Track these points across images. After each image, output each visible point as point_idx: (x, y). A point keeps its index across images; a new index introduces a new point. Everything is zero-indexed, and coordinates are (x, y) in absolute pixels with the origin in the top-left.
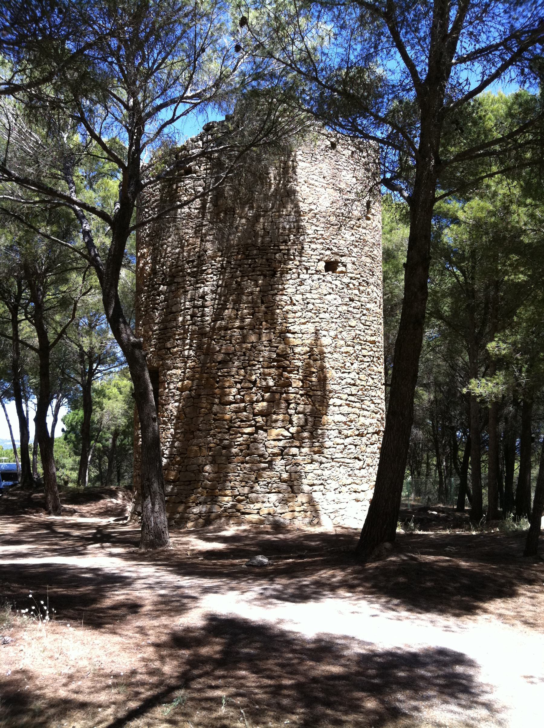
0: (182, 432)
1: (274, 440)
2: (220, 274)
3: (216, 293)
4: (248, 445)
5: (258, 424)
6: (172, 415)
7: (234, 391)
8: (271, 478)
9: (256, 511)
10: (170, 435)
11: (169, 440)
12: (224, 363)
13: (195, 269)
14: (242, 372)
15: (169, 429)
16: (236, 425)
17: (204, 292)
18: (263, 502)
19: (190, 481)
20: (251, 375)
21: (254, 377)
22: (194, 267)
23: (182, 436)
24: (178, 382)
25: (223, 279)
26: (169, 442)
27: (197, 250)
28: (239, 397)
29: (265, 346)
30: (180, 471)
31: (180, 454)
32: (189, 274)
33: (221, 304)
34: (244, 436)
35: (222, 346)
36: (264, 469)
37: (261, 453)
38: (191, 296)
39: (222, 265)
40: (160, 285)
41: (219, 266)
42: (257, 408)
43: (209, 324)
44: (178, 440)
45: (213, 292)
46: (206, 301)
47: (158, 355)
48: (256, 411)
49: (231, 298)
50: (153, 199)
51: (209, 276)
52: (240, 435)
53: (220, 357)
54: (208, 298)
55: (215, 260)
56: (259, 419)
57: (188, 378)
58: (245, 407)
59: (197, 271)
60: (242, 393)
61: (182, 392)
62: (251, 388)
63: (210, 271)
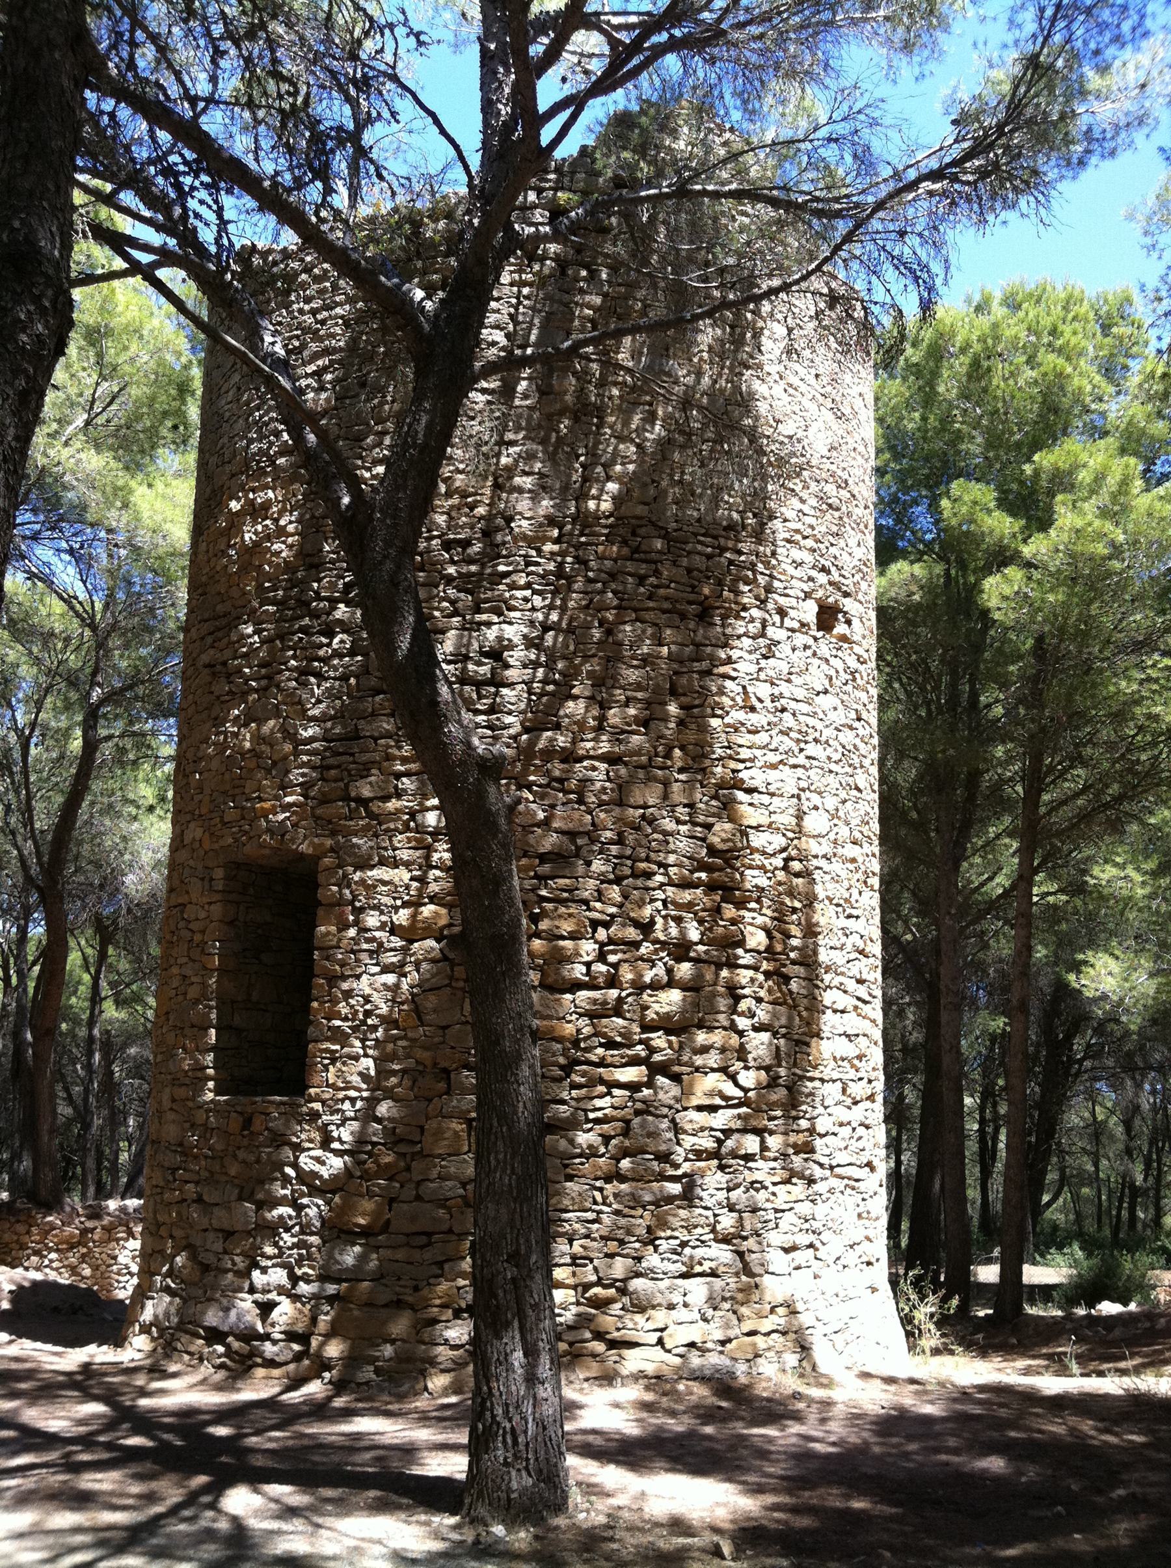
0: (404, 1071)
1: (700, 1108)
2: (555, 593)
3: (538, 647)
4: (627, 1122)
5: (657, 1058)
6: (368, 1014)
7: (588, 948)
8: (689, 1228)
9: (653, 1338)
10: (356, 1080)
11: (353, 1093)
12: (561, 860)
13: (473, 568)
14: (614, 892)
15: (356, 1058)
16: (594, 1058)
17: (500, 639)
18: (671, 1307)
19: (430, 1234)
20: (641, 904)
21: (647, 911)
22: (470, 561)
23: (407, 1082)
24: (396, 909)
25: (563, 609)
26: (353, 1101)
27: (481, 510)
28: (603, 968)
29: (679, 822)
30: (392, 1201)
31: (395, 1143)
32: (449, 580)
33: (555, 682)
34: (616, 1092)
35: (553, 806)
36: (670, 1199)
37: (663, 1147)
38: (458, 646)
39: (560, 566)
40: (334, 602)
41: (551, 566)
42: (656, 1007)
43: (515, 738)
44: (389, 1094)
45: (529, 643)
46: (507, 666)
47: (317, 818)
48: (651, 1015)
49: (588, 667)
50: (314, 347)
51: (519, 594)
52: (602, 1089)
53: (550, 842)
54: (515, 657)
55: (539, 551)
56: (659, 1040)
57: (433, 899)
58: (620, 1000)
59: (480, 573)
60: (612, 958)
61: (411, 941)
62: (636, 945)
63: (522, 580)
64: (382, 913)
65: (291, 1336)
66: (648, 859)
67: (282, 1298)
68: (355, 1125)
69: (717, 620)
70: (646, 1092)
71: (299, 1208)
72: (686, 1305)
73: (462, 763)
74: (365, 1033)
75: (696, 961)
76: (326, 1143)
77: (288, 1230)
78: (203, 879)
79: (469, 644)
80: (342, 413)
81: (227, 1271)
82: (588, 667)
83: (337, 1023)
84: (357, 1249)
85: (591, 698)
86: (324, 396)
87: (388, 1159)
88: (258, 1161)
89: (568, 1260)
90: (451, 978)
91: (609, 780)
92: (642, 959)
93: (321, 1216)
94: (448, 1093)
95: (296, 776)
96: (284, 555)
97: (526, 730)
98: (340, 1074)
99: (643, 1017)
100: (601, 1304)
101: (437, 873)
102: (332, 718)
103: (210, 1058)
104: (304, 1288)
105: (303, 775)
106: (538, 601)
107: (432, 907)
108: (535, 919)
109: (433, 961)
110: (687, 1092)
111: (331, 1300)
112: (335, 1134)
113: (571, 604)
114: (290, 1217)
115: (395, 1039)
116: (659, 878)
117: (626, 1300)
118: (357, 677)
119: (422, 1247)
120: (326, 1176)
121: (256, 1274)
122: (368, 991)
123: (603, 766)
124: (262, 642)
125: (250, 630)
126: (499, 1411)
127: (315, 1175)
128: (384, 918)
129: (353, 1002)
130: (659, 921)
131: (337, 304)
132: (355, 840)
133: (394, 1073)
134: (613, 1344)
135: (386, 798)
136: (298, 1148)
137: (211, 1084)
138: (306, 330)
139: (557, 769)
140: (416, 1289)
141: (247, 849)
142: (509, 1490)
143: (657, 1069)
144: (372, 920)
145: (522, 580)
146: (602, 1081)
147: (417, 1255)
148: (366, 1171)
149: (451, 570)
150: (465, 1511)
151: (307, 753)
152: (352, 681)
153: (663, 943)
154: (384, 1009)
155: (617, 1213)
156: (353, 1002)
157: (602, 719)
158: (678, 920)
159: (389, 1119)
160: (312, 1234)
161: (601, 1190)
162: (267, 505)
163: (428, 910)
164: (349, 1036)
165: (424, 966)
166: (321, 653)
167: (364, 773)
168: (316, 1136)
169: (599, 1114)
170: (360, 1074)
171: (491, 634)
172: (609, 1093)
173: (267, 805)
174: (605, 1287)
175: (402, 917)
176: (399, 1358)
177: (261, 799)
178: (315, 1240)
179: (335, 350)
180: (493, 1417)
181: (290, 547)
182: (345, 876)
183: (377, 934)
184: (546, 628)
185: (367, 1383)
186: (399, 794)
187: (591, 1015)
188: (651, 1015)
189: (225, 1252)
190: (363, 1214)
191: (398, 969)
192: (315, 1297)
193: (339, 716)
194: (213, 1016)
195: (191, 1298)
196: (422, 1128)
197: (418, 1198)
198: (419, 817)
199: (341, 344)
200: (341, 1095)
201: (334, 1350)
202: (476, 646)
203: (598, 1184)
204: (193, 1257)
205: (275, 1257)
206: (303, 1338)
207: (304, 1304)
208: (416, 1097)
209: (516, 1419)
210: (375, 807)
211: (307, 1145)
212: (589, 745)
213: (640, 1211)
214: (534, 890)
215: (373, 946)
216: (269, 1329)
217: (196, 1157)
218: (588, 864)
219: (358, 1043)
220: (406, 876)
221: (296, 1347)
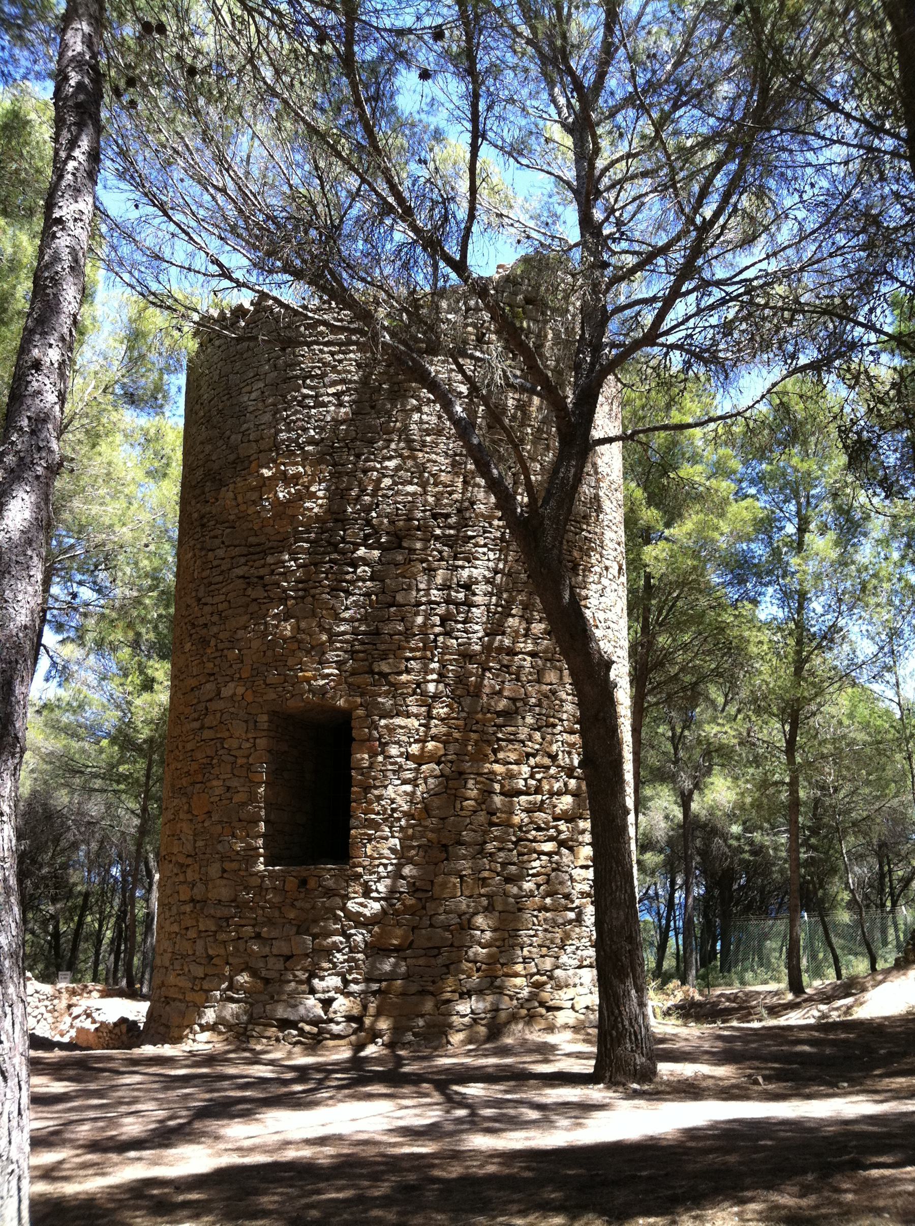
0: (419, 846)
1: (582, 867)
2: (500, 550)
3: (491, 583)
4: (548, 875)
5: (562, 836)
6: (394, 810)
7: (525, 770)
8: (579, 939)
9: (568, 1004)
10: (386, 852)
11: (385, 861)
12: (510, 715)
13: (452, 532)
14: (537, 736)
15: (386, 839)
16: (531, 837)
17: (470, 577)
18: (575, 986)
19: (439, 948)
20: (551, 743)
21: (554, 747)
22: (450, 528)
23: (421, 853)
24: (410, 744)
25: (506, 561)
26: (385, 866)
27: (455, 496)
28: (534, 782)
29: (568, 694)
30: (414, 929)
31: (415, 892)
32: (437, 538)
33: (501, 606)
34: (543, 857)
35: (503, 682)
36: (570, 922)
37: (566, 891)
38: (445, 580)
39: (503, 534)
40: (357, 546)
41: (498, 534)
42: (560, 806)
43: (480, 639)
44: (410, 861)
45: (488, 581)
46: (474, 594)
47: (350, 685)
48: (558, 811)
49: (520, 597)
50: (334, 376)
51: (481, 550)
52: (535, 856)
53: (503, 704)
54: (480, 588)
55: (491, 525)
56: (562, 825)
57: (434, 738)
58: (542, 802)
59: (457, 536)
60: (538, 776)
61: (420, 765)
62: (548, 768)
63: (481, 541)
64: (401, 746)
65: (349, 1019)
66: (554, 717)
67: (338, 995)
68: (388, 881)
69: (581, 572)
70: (556, 858)
71: (348, 937)
72: (581, 985)
73: (598, 664)
74: (392, 822)
75: (577, 778)
76: (367, 893)
77: (339, 951)
78: (246, 722)
79: (452, 579)
80: (358, 423)
81: (290, 981)
82: (520, 597)
83: (373, 816)
84: (392, 960)
85: (521, 617)
86: (343, 410)
87: (411, 902)
88: (313, 908)
89: (521, 960)
90: (446, 787)
91: (532, 667)
92: (552, 777)
93: (365, 941)
94: (447, 859)
95: (331, 656)
96: (315, 510)
97: (487, 635)
98: (375, 849)
99: (554, 812)
100: (539, 986)
101: (436, 722)
102: (358, 620)
103: (260, 842)
104: (354, 987)
105: (337, 656)
106: (491, 555)
107: (433, 743)
108: (495, 752)
109: (436, 777)
110: (576, 857)
111: (374, 993)
112: (374, 887)
113: (510, 558)
114: (341, 943)
115: (413, 826)
116: (559, 728)
117: (552, 982)
118: (376, 595)
119: (435, 956)
120: (368, 914)
121: (316, 981)
122: (393, 796)
123: (529, 659)
124: (299, 567)
125: (287, 557)
126: (626, 1023)
127: (359, 914)
128: (402, 750)
129: (383, 803)
130: (560, 753)
131: (351, 351)
132: (380, 699)
133: (413, 847)
134: (550, 1009)
135: (400, 673)
136: (347, 897)
137: (262, 859)
138: (325, 364)
139: (506, 659)
140: (434, 982)
141: (291, 703)
142: (635, 1064)
143: (562, 844)
144: (394, 750)
145: (481, 541)
146: (535, 851)
147: (433, 961)
148: (396, 910)
149: (438, 532)
150: (607, 1080)
151: (341, 642)
152: (374, 597)
153: (563, 767)
154: (405, 808)
155: (546, 930)
156: (383, 803)
157: (527, 630)
158: (569, 753)
159: (411, 877)
160: (359, 952)
161: (536, 917)
162: (297, 476)
163: (430, 745)
164: (380, 824)
165: (430, 780)
166: (348, 577)
167: (384, 657)
168: (358, 888)
169: (534, 871)
170: (389, 849)
171: (465, 573)
172: (539, 858)
173: (309, 674)
174: (542, 975)
175: (415, 749)
176: (428, 1025)
177: (302, 670)
178: (360, 956)
179: (350, 382)
180: (624, 1026)
181: (321, 506)
182: (373, 722)
183: (399, 760)
184: (496, 572)
185: (409, 1043)
186: (408, 671)
187: (527, 811)
188: (558, 811)
189: (286, 969)
190: (396, 938)
191: (413, 782)
192: (363, 992)
193: (364, 619)
194: (263, 813)
195: (257, 1002)
196: (432, 882)
197: (431, 926)
198: (423, 686)
199: (356, 378)
200: (377, 862)
201: (383, 1025)
202: (455, 580)
203: (535, 913)
204: (254, 973)
205: (330, 969)
206: (358, 1019)
207: (355, 998)
208: (427, 863)
209: (636, 1027)
210: (392, 678)
211: (353, 895)
212: (522, 645)
213: (557, 929)
214: (494, 733)
215: (396, 767)
216: (332, 1015)
217: (251, 908)
218: (524, 718)
219: (387, 829)
220: (416, 723)
221: (354, 1025)
